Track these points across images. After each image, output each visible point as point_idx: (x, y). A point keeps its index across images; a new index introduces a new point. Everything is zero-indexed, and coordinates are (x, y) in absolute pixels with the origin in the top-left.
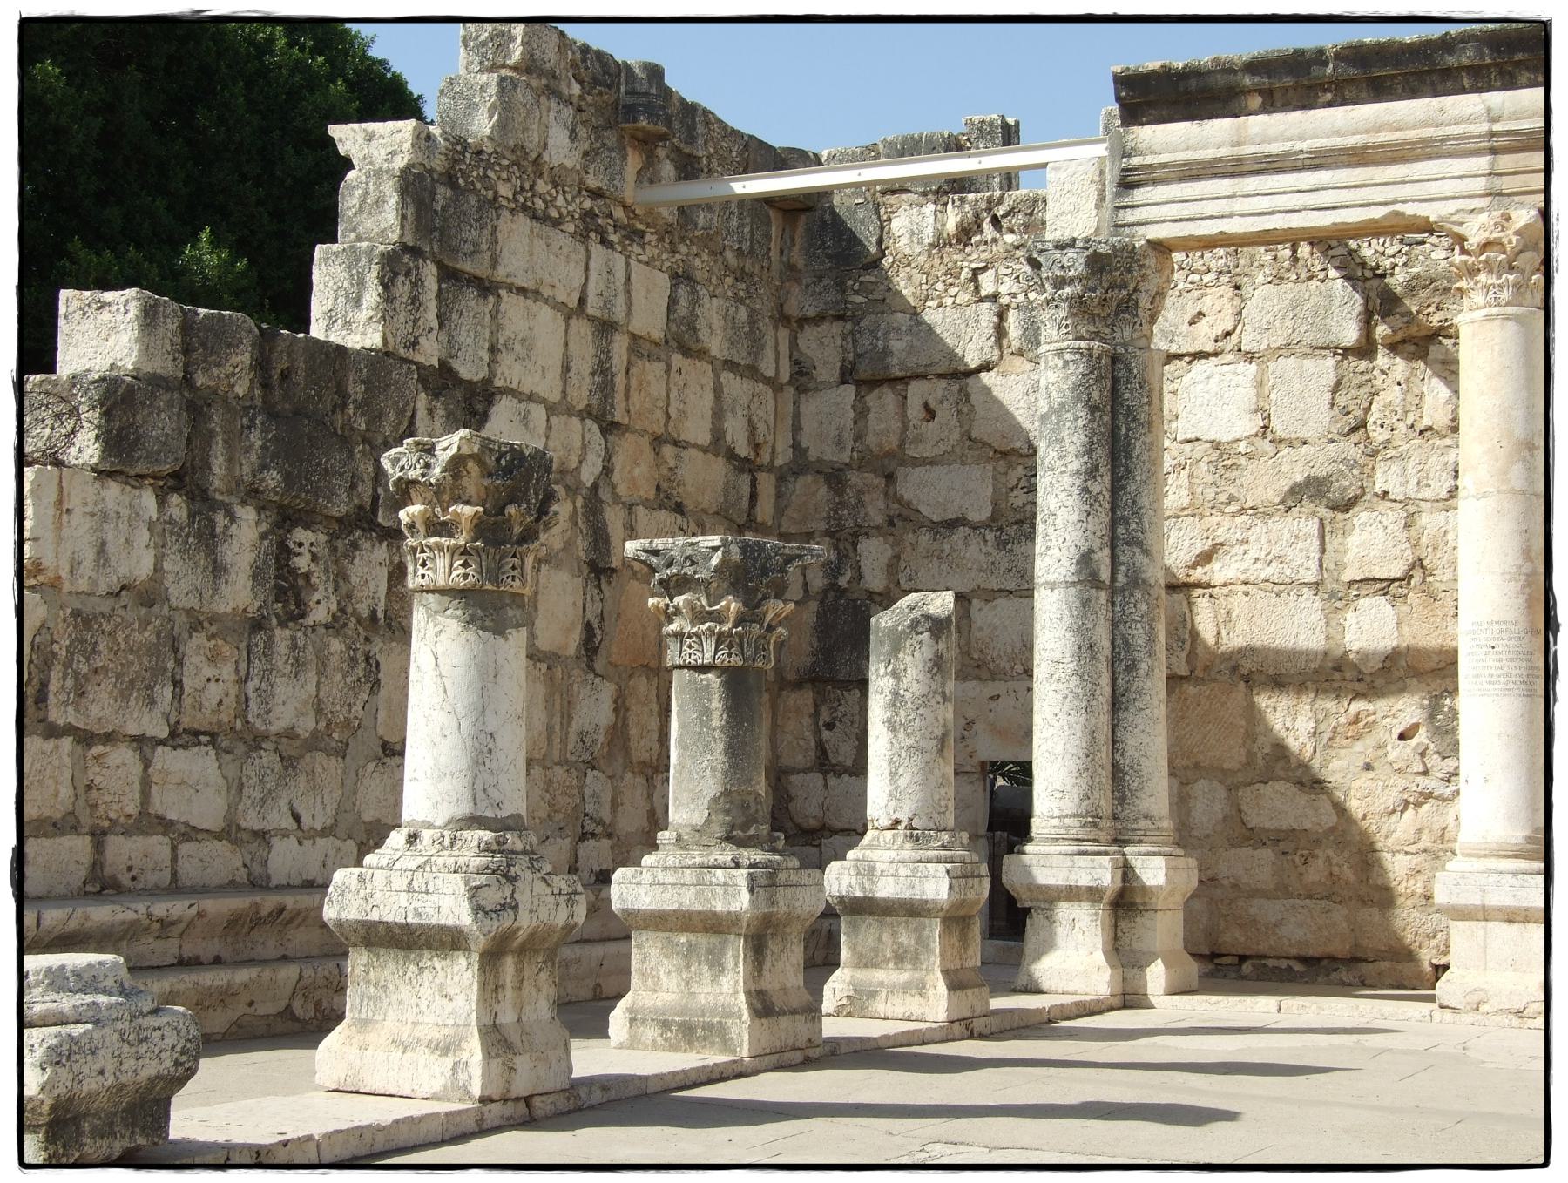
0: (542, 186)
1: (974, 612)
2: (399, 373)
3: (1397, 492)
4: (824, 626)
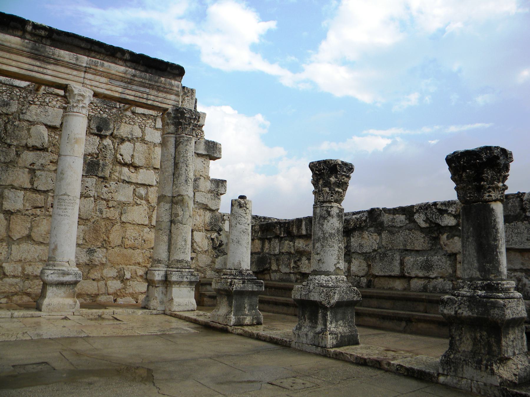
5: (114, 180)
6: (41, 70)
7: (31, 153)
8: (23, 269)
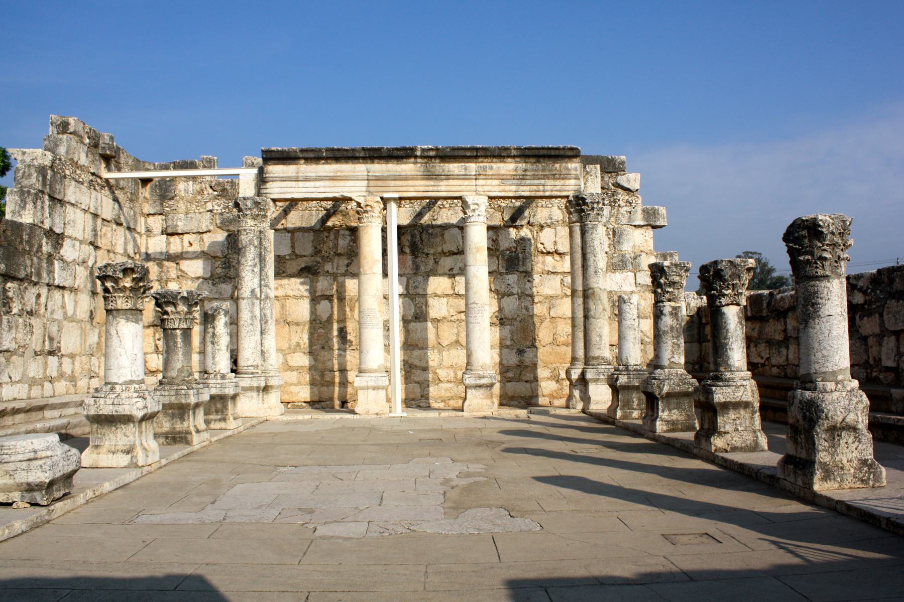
0: (78, 172)
2: (38, 232)
5: (538, 273)
6: (435, 188)
7: (449, 258)
8: (456, 374)
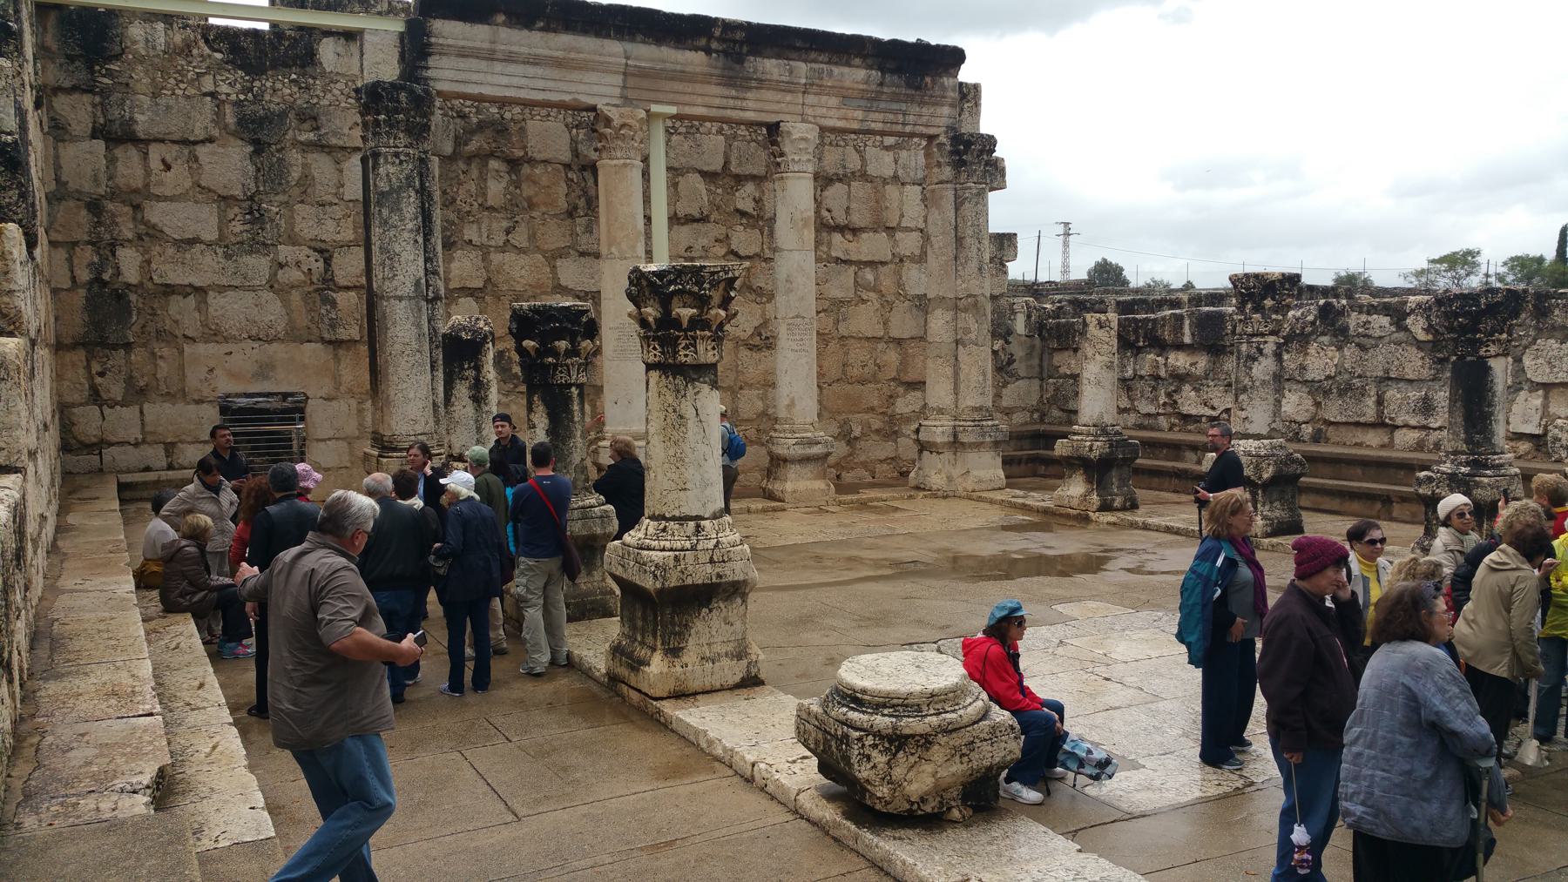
1: (210, 299)
3: (475, 240)
4: (92, 305)
6: (738, 103)
